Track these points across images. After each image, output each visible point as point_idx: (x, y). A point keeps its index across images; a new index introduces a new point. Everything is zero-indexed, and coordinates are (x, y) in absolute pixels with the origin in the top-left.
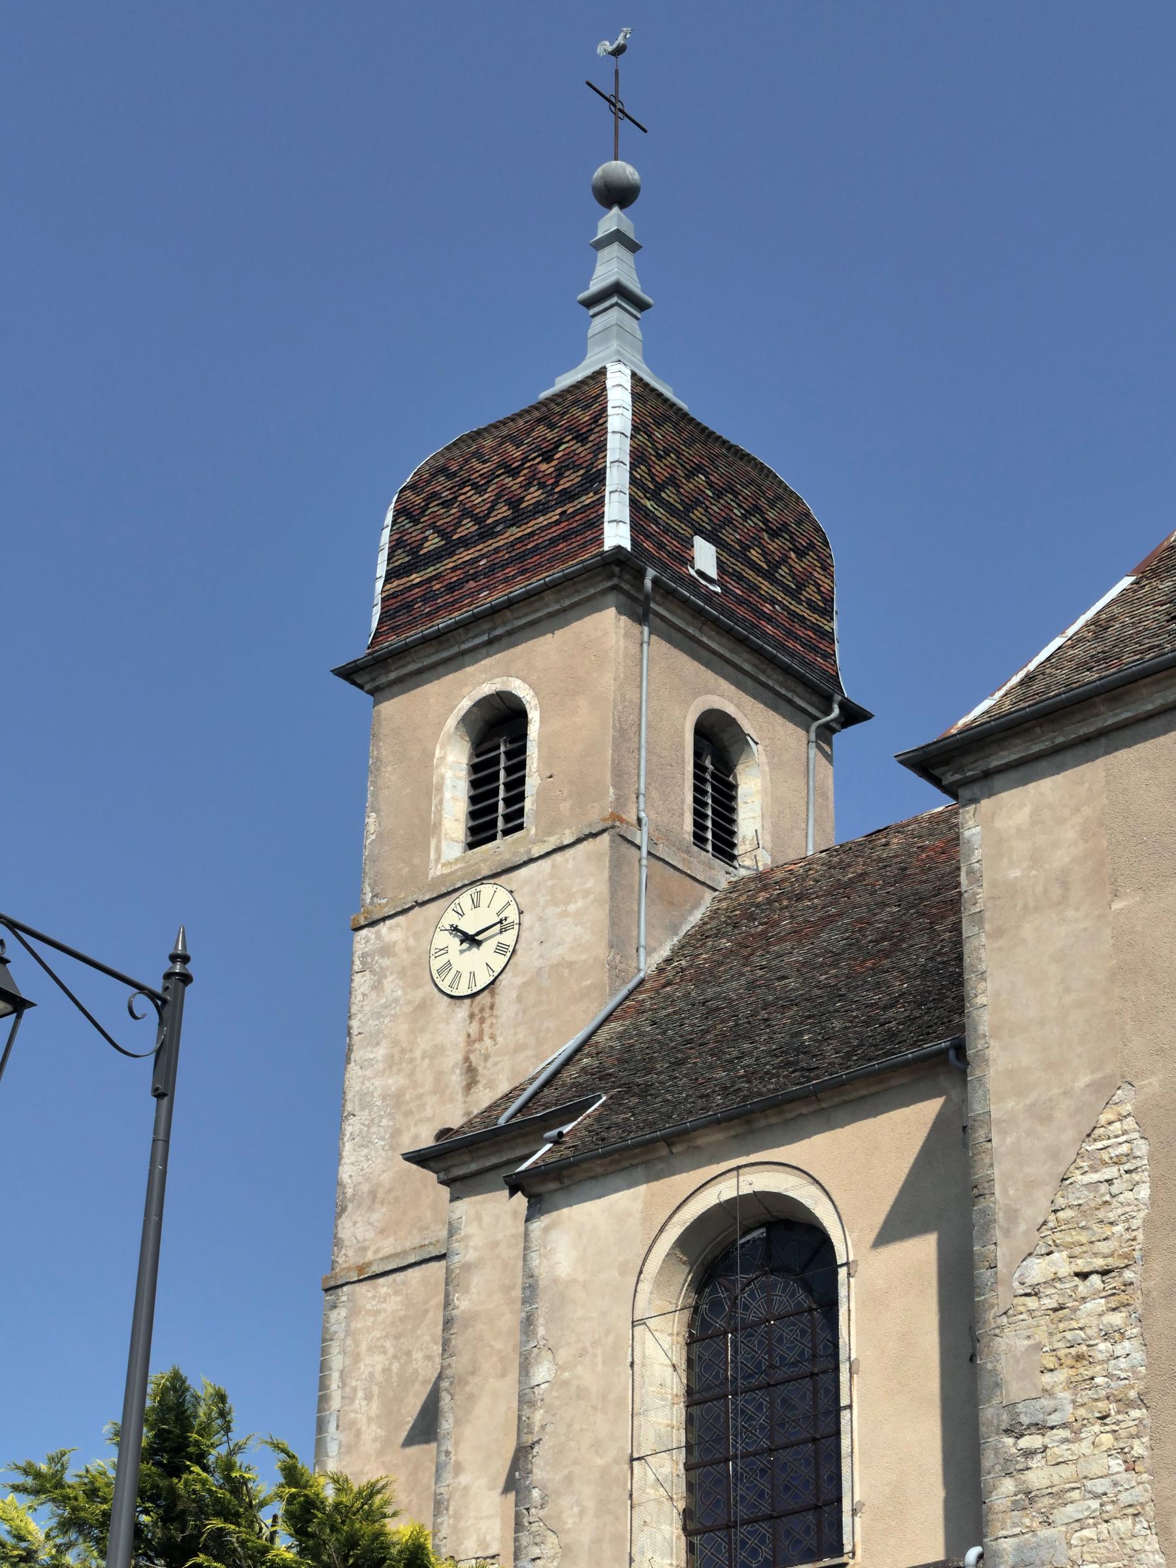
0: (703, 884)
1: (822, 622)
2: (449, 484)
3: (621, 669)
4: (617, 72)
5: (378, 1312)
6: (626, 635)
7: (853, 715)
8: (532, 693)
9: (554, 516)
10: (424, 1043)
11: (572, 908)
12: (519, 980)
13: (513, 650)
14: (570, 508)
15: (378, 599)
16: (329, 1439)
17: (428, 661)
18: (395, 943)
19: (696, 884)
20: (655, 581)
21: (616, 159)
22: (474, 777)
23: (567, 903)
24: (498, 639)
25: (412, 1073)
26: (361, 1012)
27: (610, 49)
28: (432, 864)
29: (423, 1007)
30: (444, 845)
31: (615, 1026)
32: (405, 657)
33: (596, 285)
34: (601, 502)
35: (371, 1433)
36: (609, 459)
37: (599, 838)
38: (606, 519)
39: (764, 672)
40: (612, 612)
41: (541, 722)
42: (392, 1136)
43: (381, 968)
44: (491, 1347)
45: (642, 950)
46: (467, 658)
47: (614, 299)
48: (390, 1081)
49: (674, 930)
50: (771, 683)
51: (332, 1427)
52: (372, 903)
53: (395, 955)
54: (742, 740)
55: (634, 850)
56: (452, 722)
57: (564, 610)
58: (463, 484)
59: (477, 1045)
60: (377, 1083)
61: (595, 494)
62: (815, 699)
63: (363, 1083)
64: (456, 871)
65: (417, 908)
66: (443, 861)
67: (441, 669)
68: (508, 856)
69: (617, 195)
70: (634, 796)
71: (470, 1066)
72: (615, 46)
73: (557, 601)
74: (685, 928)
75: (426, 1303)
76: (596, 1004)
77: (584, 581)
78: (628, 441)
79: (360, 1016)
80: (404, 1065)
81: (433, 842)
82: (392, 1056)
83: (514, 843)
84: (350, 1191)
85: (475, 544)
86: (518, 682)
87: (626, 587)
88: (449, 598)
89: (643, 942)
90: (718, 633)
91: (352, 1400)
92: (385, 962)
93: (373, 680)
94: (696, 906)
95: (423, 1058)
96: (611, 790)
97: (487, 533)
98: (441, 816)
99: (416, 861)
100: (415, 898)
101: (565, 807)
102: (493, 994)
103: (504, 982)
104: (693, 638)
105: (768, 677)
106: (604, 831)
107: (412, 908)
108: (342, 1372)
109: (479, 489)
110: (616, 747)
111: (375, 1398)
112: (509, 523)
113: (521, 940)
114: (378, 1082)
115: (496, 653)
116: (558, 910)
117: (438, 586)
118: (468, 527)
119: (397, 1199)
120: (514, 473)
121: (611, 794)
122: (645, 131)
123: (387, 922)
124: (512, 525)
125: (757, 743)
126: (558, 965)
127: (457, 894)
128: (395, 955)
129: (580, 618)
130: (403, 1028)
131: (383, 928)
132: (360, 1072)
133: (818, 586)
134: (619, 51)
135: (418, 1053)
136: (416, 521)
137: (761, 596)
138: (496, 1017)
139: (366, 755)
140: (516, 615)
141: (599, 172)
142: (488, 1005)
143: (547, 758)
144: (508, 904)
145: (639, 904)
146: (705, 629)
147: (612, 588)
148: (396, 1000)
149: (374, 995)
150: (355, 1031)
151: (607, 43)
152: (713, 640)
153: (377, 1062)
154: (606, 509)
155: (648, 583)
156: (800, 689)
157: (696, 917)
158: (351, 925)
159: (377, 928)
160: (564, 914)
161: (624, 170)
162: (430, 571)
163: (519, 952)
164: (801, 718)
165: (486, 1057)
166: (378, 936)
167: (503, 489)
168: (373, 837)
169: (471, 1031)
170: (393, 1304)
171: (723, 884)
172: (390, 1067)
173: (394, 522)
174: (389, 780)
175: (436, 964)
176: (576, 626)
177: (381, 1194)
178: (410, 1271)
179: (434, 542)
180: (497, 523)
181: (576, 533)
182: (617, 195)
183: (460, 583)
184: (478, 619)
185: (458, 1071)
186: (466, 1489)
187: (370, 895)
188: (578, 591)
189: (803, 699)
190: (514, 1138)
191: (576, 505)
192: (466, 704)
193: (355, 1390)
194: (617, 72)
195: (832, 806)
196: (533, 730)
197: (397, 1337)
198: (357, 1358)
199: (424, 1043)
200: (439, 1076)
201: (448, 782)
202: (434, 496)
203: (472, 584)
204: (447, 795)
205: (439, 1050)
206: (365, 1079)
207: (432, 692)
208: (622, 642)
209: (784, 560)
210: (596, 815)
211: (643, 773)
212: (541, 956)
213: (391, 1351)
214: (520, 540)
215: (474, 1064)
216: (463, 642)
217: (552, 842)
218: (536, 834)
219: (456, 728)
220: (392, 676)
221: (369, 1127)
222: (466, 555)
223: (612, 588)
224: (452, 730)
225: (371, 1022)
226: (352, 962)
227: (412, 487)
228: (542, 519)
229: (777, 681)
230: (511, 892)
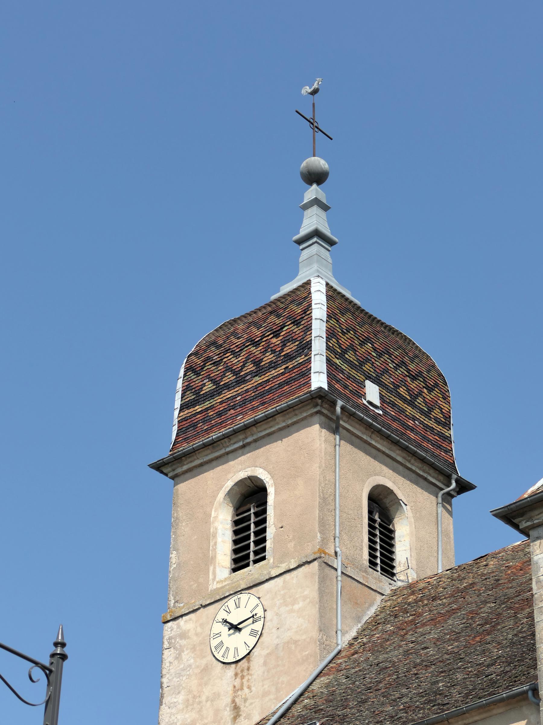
0: (375, 591)
1: (444, 430)
2: (217, 352)
3: (323, 461)
4: (314, 104)
6: (325, 441)
7: (464, 487)
8: (269, 477)
9: (281, 370)
10: (207, 692)
11: (296, 607)
12: (265, 652)
13: (257, 451)
14: (290, 365)
15: (176, 421)
17: (206, 459)
18: (189, 630)
19: (371, 591)
20: (343, 408)
21: (314, 156)
22: (235, 528)
23: (293, 605)
24: (249, 444)
25: (200, 711)
26: (168, 673)
27: (310, 91)
28: (211, 582)
29: (206, 670)
30: (218, 570)
31: (324, 680)
32: (193, 456)
33: (304, 231)
34: (309, 361)
36: (313, 335)
37: (311, 564)
38: (312, 371)
39: (409, 461)
40: (317, 427)
41: (275, 494)
43: (180, 646)
45: (339, 632)
46: (230, 456)
47: (315, 239)
48: (187, 716)
49: (358, 619)
50: (414, 468)
52: (174, 606)
53: (189, 638)
54: (397, 501)
55: (333, 571)
56: (221, 495)
57: (288, 426)
58: (227, 351)
59: (239, 693)
60: (179, 717)
61: (306, 356)
62: (441, 478)
63: (170, 717)
64: (225, 585)
66: (217, 580)
67: (214, 463)
68: (256, 576)
69: (316, 177)
70: (333, 538)
71: (236, 705)
72: (312, 89)
73: (284, 421)
74: (365, 619)
76: (311, 666)
77: (300, 408)
78: (325, 324)
79: (168, 676)
80: (195, 705)
81: (211, 568)
82: (188, 700)
83: (260, 568)
85: (234, 387)
86: (261, 470)
87: (325, 411)
88: (218, 420)
89: (339, 627)
90: (381, 439)
92: (183, 642)
93: (174, 470)
94: (371, 605)
95: (207, 701)
96: (319, 535)
97: (240, 381)
98: (216, 553)
99: (201, 580)
100: (201, 602)
101: (291, 545)
102: (249, 661)
103: (255, 654)
104: (366, 442)
105: (413, 464)
106: (315, 560)
109: (236, 354)
110: (321, 509)
112: (254, 374)
113: (265, 627)
115: (248, 453)
116: (287, 609)
117: (212, 413)
118: (230, 377)
120: (256, 344)
121: (319, 537)
122: (331, 139)
123: (184, 618)
124: (256, 376)
125: (406, 505)
126: (288, 642)
128: (189, 638)
129: (298, 431)
130: (194, 683)
131: (181, 621)
132: (169, 711)
133: (441, 409)
134: (315, 92)
135: (204, 698)
136: (198, 374)
137: (406, 416)
138: (251, 675)
139: (170, 516)
140: (259, 430)
141: (304, 164)
142: (246, 668)
143: (280, 516)
144: (257, 605)
145: (337, 604)
146: (373, 436)
147: (317, 412)
148: (190, 666)
149: (176, 662)
150: (165, 685)
151: (308, 87)
152: (379, 443)
153: (179, 704)
154: (312, 365)
155: (338, 409)
156: (432, 471)
157: (371, 612)
158: (162, 620)
159: (177, 621)
160: (292, 611)
161: (319, 162)
162: (207, 404)
164: (434, 489)
165: (245, 700)
166: (179, 626)
167: (250, 354)
168: (175, 566)
169: (236, 684)
171: (387, 591)
172: (187, 707)
173: (185, 375)
174: (184, 532)
175: (214, 643)
176: (296, 436)
179: (209, 387)
180: (247, 374)
181: (295, 380)
182: (316, 177)
183: (226, 411)
184: (236, 433)
185: (228, 709)
187: (173, 601)
188: (296, 415)
189: (433, 477)
191: (294, 363)
192: (230, 484)
194: (314, 104)
195: (452, 542)
196: (271, 499)
199: (207, 692)
200: (217, 712)
201: (220, 532)
202: (209, 359)
203: (232, 411)
204: (219, 539)
205: (216, 696)
206: (171, 714)
207: (209, 477)
208: (323, 445)
209: (420, 394)
210: (309, 551)
211: (337, 524)
212: (278, 637)
214: (261, 384)
215: (238, 704)
216: (228, 446)
217: (284, 567)
218: (274, 563)
219: (224, 499)
220: (185, 468)
222: (228, 394)
223: (317, 412)
224: (222, 500)
225: (175, 679)
226: (163, 643)
227: (196, 354)
228: (274, 371)
229: (417, 467)
230: (259, 598)
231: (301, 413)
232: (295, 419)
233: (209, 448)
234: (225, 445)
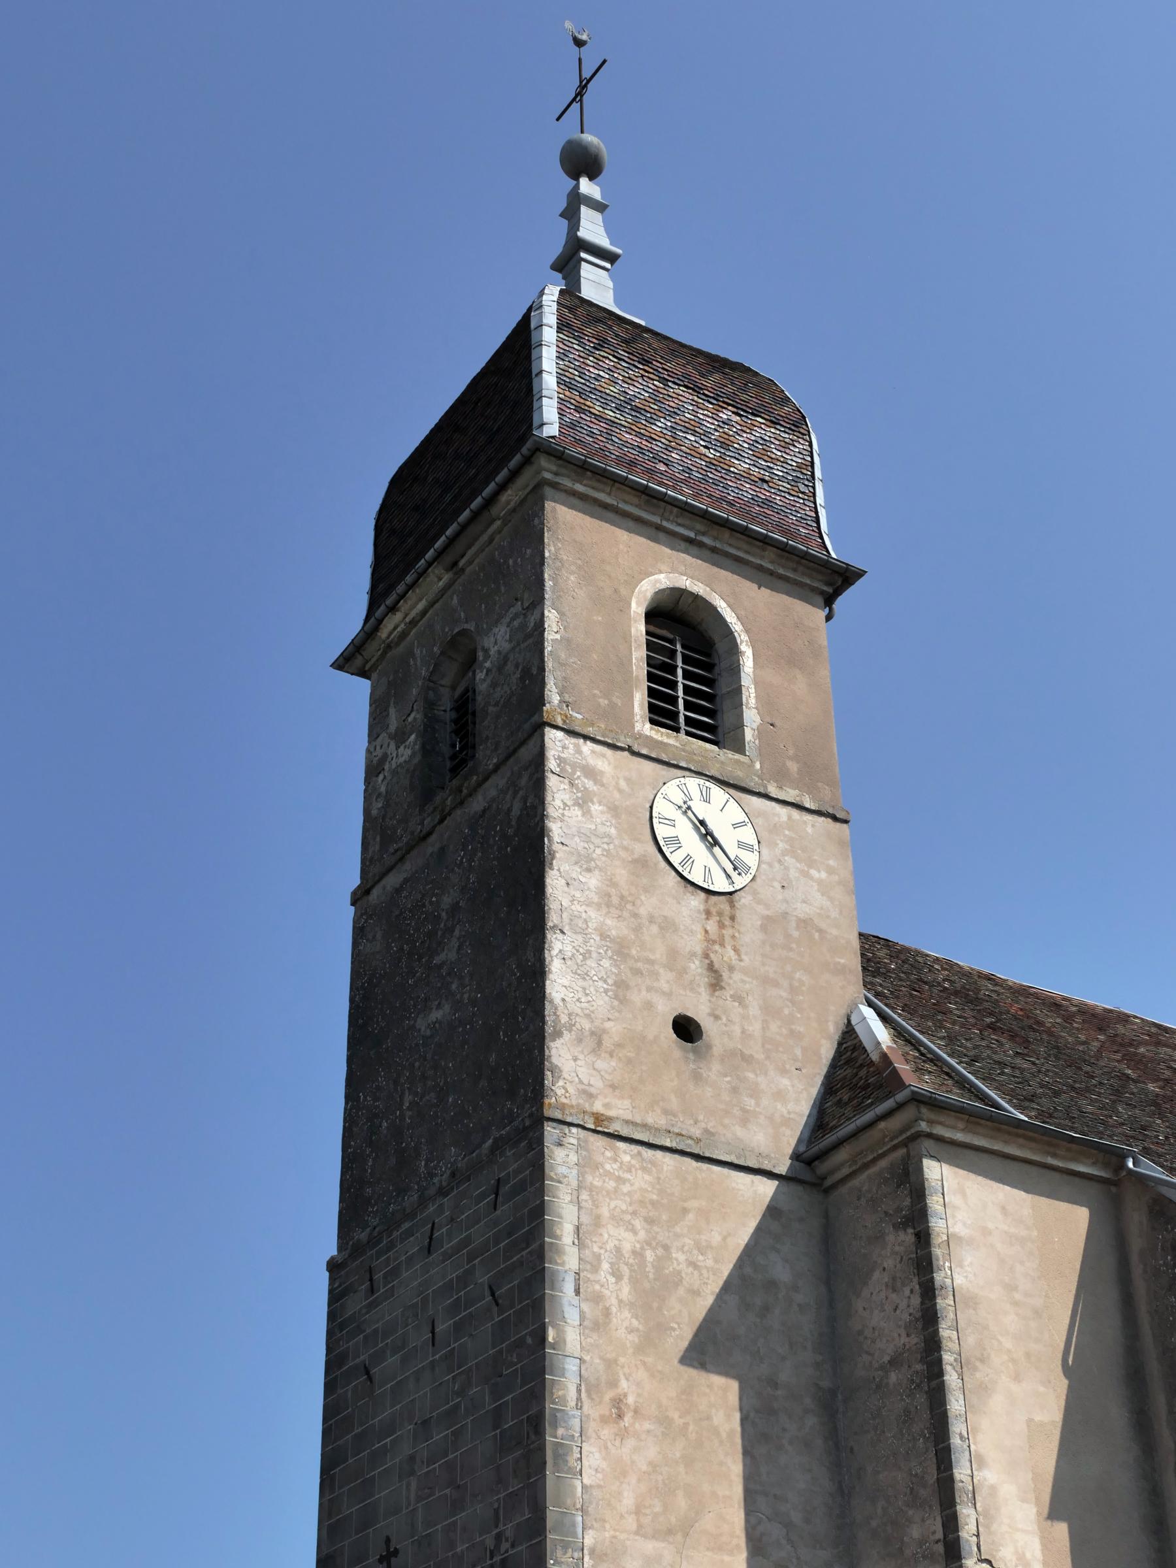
4: (580, 60)
5: (620, 1180)
10: (647, 905)
11: (813, 872)
16: (565, 1301)
29: (641, 863)
32: (605, 484)
35: (624, 1322)
42: (615, 983)
44: (1000, 1343)
46: (661, 535)
51: (568, 1287)
57: (772, 573)
65: (626, 753)
73: (772, 562)
75: (685, 1201)
77: (808, 568)
84: (564, 1019)
91: (596, 1269)
92: (590, 784)
93: (556, 474)
107: (622, 749)
108: (578, 1228)
111: (626, 1279)
114: (592, 913)
119: (629, 1061)
122: (558, 119)
127: (687, 773)
143: (766, 704)
147: (822, 593)
149: (577, 812)
163: (758, 880)
165: (731, 969)
170: (640, 1181)
177: (607, 1043)
178: (659, 1154)
186: (993, 1489)
188: (795, 570)
190: (1018, 1135)
193: (598, 1257)
194: (580, 60)
197: (650, 1221)
198: (597, 1222)
200: (673, 954)
213: (642, 1235)
215: (716, 966)
216: (668, 520)
220: (579, 488)
221: (585, 958)
231: (803, 574)
232: (790, 574)
233: (639, 497)
234: (667, 514)
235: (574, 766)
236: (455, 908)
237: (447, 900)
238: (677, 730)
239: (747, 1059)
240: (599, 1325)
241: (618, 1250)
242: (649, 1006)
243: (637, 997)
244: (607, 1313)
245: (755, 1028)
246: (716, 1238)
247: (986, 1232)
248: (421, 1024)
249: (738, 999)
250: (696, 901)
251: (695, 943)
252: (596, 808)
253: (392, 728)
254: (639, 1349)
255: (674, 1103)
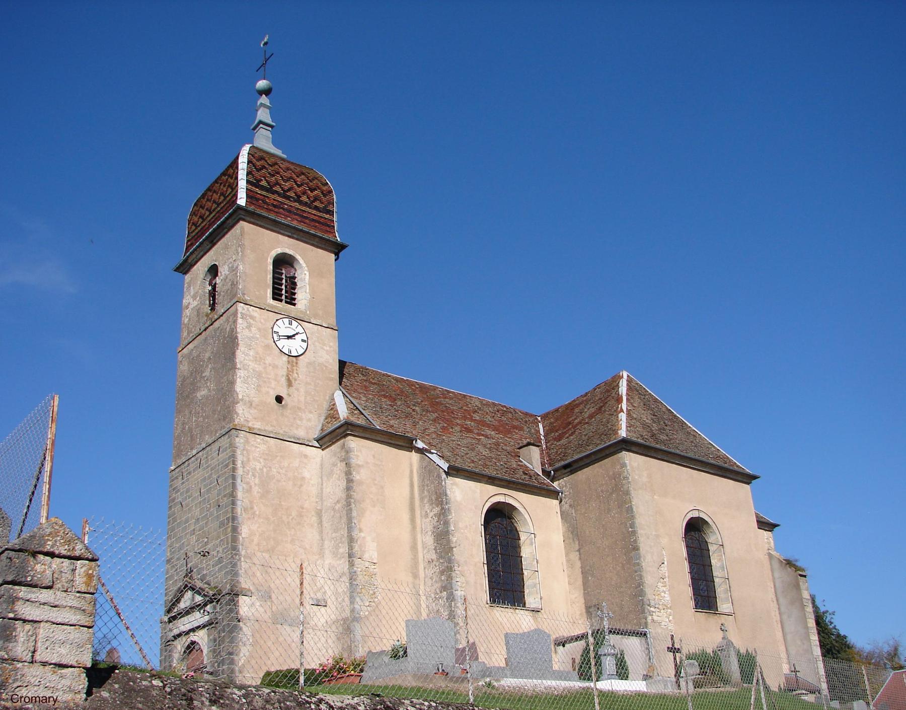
29: (267, 347)
51: (239, 480)
84: (240, 397)
92: (251, 321)
165: (296, 380)
170: (263, 447)
235: (246, 315)
236: (210, 358)
237: (207, 355)
238: (281, 301)
239: (299, 408)
240: (249, 490)
241: (255, 469)
242: (268, 393)
243: (264, 390)
244: (251, 487)
245: (302, 399)
246: (286, 464)
247: (367, 463)
248: (198, 395)
249: (297, 390)
250: (285, 358)
251: (284, 372)
252: (253, 329)
253: (192, 294)
254: (261, 498)
255: (275, 423)
